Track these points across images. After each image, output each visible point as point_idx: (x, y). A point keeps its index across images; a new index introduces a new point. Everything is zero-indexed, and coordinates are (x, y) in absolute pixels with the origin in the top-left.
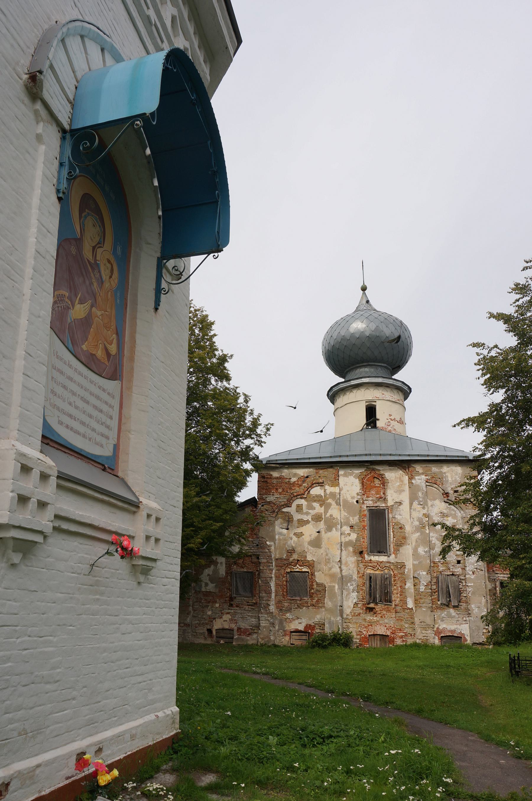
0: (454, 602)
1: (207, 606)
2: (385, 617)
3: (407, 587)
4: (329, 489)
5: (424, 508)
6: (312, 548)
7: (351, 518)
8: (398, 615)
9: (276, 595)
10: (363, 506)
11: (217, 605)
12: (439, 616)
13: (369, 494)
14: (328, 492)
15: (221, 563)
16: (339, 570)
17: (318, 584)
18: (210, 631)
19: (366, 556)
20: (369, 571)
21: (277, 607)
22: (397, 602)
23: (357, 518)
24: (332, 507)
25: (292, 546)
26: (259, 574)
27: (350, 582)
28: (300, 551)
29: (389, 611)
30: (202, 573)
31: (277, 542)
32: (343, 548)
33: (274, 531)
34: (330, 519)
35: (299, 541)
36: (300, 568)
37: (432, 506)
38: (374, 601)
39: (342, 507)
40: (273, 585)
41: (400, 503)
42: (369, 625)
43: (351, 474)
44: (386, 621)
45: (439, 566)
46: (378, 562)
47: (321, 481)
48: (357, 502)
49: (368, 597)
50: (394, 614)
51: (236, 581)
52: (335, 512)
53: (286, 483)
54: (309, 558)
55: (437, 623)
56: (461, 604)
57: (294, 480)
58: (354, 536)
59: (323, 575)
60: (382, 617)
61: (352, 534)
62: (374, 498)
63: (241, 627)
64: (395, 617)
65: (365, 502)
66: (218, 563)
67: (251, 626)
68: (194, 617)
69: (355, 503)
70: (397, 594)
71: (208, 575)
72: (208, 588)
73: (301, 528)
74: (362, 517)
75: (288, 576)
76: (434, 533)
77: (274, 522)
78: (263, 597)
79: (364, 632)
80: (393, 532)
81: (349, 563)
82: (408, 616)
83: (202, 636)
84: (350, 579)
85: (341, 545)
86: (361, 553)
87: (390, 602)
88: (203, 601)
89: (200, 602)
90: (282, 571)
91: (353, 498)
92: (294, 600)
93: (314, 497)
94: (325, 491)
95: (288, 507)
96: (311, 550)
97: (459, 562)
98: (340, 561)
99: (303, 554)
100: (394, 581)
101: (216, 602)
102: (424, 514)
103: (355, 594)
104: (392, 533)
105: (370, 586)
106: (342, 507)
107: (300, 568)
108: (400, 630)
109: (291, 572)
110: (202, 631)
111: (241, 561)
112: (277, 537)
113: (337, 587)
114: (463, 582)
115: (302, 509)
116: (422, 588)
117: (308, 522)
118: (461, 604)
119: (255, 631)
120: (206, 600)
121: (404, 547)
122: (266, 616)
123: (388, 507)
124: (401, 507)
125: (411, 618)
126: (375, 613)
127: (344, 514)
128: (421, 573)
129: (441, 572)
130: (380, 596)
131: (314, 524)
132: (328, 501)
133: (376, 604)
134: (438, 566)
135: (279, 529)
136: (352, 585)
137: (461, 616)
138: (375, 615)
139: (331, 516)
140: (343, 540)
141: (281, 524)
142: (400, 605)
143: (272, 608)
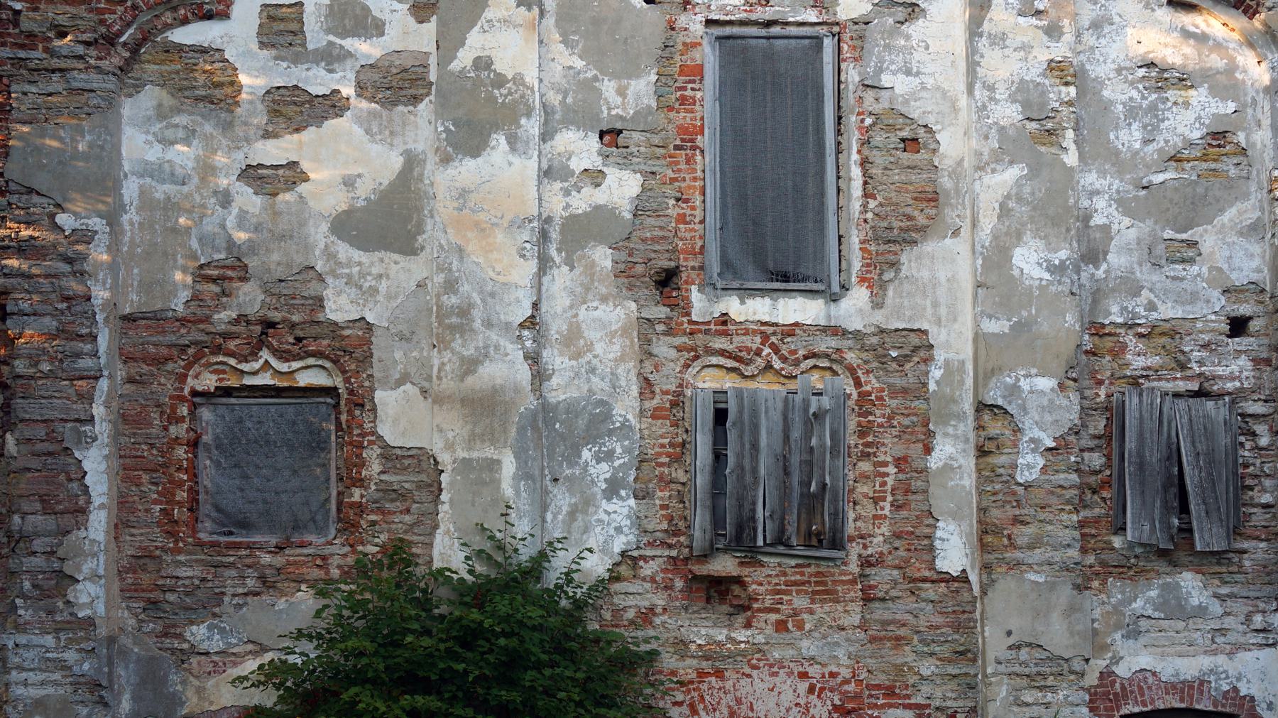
0: (1207, 536)
2: (800, 626)
3: (935, 461)
5: (1053, 32)
6: (357, 255)
7: (608, 88)
8: (879, 612)
9: (120, 526)
10: (682, 20)
16: (523, 373)
17: (391, 456)
19: (697, 298)
20: (710, 381)
21: (130, 593)
22: (877, 545)
23: (642, 89)
25: (231, 244)
27: (591, 437)
28: (280, 273)
29: (825, 592)
31: (130, 217)
32: (553, 252)
33: (108, 155)
34: (477, 82)
35: (277, 214)
36: (284, 367)
37: (1096, 26)
38: (738, 538)
39: (550, 21)
40: (96, 465)
42: (702, 674)
44: (808, 647)
45: (1124, 347)
46: (767, 332)
49: (701, 519)
50: (856, 608)
54: (340, 307)
55: (1104, 648)
56: (1246, 545)
58: (622, 188)
59: (422, 405)
60: (781, 626)
61: (613, 174)
64: (863, 626)
70: (876, 501)
74: (677, 76)
75: (206, 414)
76: (1102, 174)
77: (111, 104)
78: (24, 537)
80: (864, 163)
81: (592, 334)
82: (939, 620)
84: (596, 423)
85: (544, 236)
86: (666, 281)
87: (837, 542)
90: (165, 386)
92: (237, 546)
95: (209, 16)
97: (1238, 326)
98: (532, 322)
100: (862, 433)
102: (1055, 68)
103: (622, 509)
104: (856, 172)
105: (719, 457)
106: (550, 21)
107: (284, 367)
108: (890, 692)
109: (227, 392)
112: (130, 189)
113: (509, 466)
114: (1261, 428)
116: (1030, 465)
117: (332, 105)
118: (1246, 545)
121: (929, 247)
123: (837, 29)
124: (916, 29)
125: (957, 628)
126: (746, 608)
127: (566, 59)
128: (1025, 384)
129: (1134, 382)
133: (752, 555)
134: (1119, 351)
135: (147, 141)
136: (610, 456)
137: (1240, 608)
138: (740, 619)
139: (483, 63)
140: (557, 203)
141: (161, 114)
142: (889, 560)
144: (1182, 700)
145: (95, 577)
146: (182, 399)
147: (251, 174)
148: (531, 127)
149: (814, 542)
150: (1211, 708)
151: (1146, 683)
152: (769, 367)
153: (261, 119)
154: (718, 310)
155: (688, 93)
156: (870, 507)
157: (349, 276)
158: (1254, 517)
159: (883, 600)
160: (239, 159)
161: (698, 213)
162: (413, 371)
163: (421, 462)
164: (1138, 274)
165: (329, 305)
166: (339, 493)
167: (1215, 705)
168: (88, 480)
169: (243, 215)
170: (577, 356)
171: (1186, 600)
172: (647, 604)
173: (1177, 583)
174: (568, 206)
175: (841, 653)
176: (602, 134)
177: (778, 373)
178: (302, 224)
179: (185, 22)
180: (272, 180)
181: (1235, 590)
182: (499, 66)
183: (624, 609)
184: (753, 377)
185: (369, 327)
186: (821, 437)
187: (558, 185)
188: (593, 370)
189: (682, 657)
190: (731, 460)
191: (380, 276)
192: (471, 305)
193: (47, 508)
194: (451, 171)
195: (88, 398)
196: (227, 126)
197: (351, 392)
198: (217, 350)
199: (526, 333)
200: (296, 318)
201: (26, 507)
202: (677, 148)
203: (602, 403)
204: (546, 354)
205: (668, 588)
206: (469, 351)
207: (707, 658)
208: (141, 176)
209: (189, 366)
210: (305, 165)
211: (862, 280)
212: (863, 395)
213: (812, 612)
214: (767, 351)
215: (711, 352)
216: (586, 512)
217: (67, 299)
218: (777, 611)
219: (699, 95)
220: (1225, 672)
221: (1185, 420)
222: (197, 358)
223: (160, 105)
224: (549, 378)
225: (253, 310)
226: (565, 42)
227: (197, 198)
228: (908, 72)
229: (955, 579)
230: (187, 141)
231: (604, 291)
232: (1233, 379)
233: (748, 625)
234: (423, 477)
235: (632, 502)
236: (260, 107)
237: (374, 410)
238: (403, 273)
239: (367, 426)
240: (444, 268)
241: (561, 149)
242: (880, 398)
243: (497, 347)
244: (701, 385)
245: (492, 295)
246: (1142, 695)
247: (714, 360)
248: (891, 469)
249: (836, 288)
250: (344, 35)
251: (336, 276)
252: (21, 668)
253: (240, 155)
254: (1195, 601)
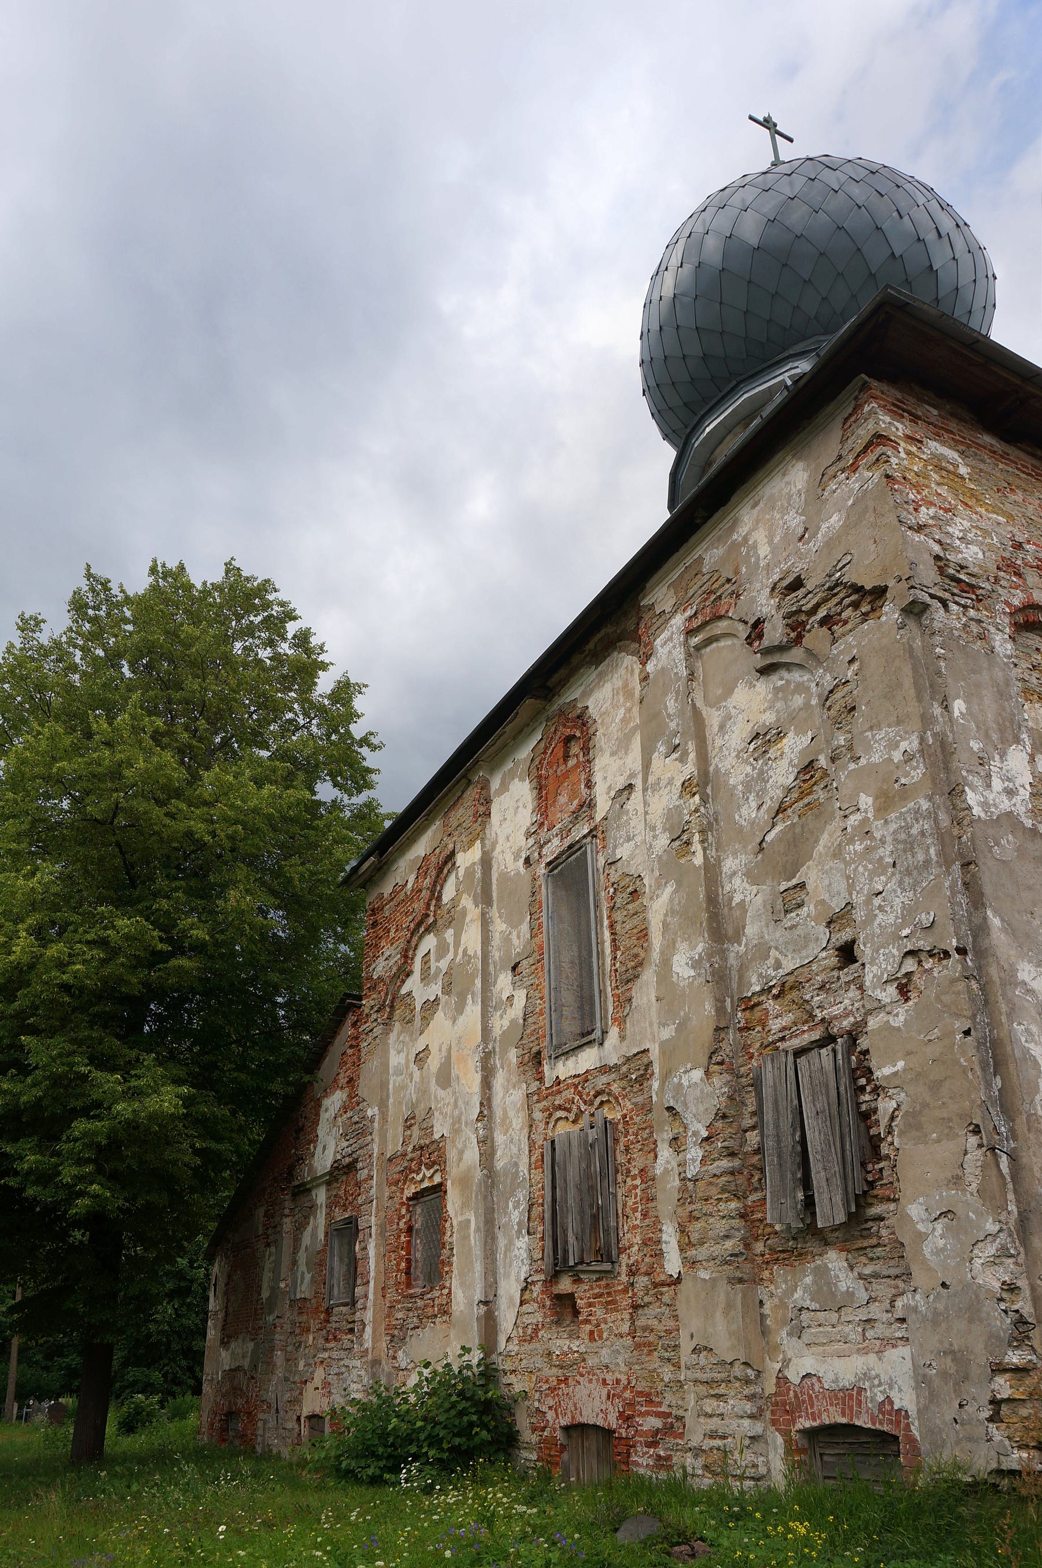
12: (783, 1305)
41: (630, 787)
144: (843, 1415)
150: (869, 1426)
151: (813, 1389)
158: (885, 1173)
164: (766, 937)
167: (874, 1424)
171: (835, 1285)
173: (826, 1264)
181: (877, 1268)
220: (878, 1376)
221: (808, 1074)
228: (629, 839)
232: (847, 1016)
246: (812, 1407)
254: (843, 1287)
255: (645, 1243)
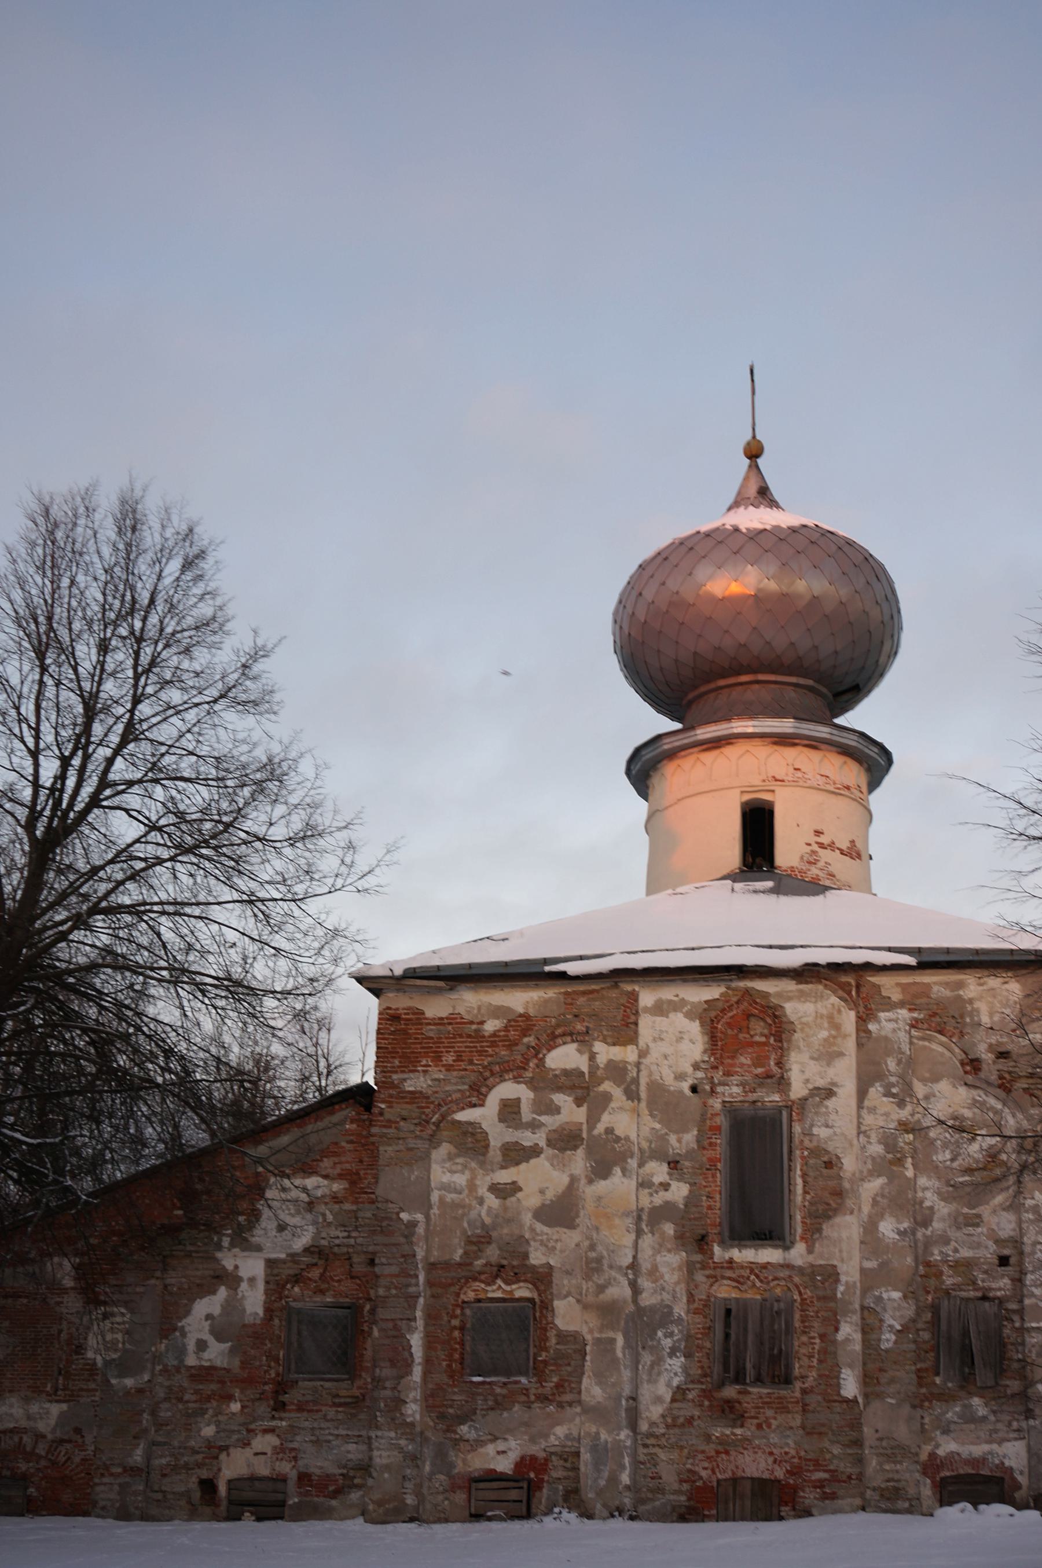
1: (203, 1412)
2: (769, 1426)
4: (605, 1052)
6: (546, 1229)
7: (673, 1139)
9: (426, 1374)
10: (711, 1101)
11: (235, 1407)
13: (732, 1065)
14: (602, 1060)
15: (252, 1280)
16: (628, 1292)
17: (563, 1337)
18: (208, 1486)
19: (717, 1249)
22: (810, 1382)
23: (690, 1138)
24: (613, 1105)
26: (372, 1312)
27: (662, 1324)
29: (782, 1407)
30: (188, 1313)
31: (435, 1211)
32: (644, 1227)
35: (506, 1209)
40: (416, 1341)
42: (718, 1452)
43: (675, 1006)
44: (774, 1438)
47: (579, 1027)
48: (694, 1089)
49: (717, 1369)
51: (299, 1333)
52: (623, 1120)
53: (469, 1036)
54: (537, 1258)
57: (491, 1026)
58: (679, 1191)
59: (578, 1307)
60: (759, 1426)
61: (674, 1185)
62: (748, 1078)
63: (312, 1470)
65: (719, 1089)
66: (240, 1279)
67: (345, 1467)
68: (154, 1443)
69: (688, 1092)
70: (810, 1357)
71: (209, 1317)
72: (206, 1355)
73: (513, 1170)
74: (707, 1132)
79: (704, 1474)
81: (663, 1270)
83: (183, 1503)
84: (663, 1316)
85: (639, 1218)
86: (702, 1242)
88: (187, 1397)
89: (180, 1400)
91: (680, 1077)
93: (556, 1076)
94: (592, 1057)
95: (475, 1106)
96: (542, 1233)
98: (634, 1266)
99: (517, 1249)
100: (803, 1322)
101: (230, 1398)
103: (676, 1363)
105: (727, 1336)
106: (643, 1104)
110: (181, 1488)
111: (315, 1273)
112: (435, 1197)
115: (519, 1113)
117: (535, 1152)
119: (357, 1481)
120: (196, 1392)
122: (392, 1434)
127: (651, 1124)
130: (757, 1368)
131: (555, 1156)
132: (601, 1088)
136: (671, 1335)
138: (739, 1422)
139: (609, 1131)
140: (645, 1201)
141: (450, 1158)
143: (413, 1410)
145: (415, 1401)
146: (457, 1306)
147: (494, 1188)
148: (633, 1163)
149: (777, 1380)
152: (754, 1285)
153: (499, 1158)
154: (727, 1256)
155: (714, 1140)
156: (806, 1359)
157: (542, 1241)
159: (813, 1412)
160: (488, 1180)
161: (718, 1205)
162: (573, 1290)
163: (573, 1338)
165: (532, 1256)
166: (535, 1354)
168: (413, 1350)
169: (490, 1208)
170: (655, 1281)
172: (690, 1414)
174: (652, 1202)
175: (790, 1442)
176: (669, 1163)
177: (758, 1288)
178: (519, 1213)
179: (463, 1109)
180: (506, 1191)
182: (617, 1132)
183: (678, 1417)
184: (746, 1291)
185: (551, 1267)
186: (780, 1324)
187: (647, 1191)
188: (663, 1289)
189: (708, 1443)
190: (733, 1337)
191: (557, 1240)
192: (602, 1257)
193: (393, 1363)
194: (593, 1187)
195: (413, 1307)
196: (482, 1164)
197: (542, 1302)
198: (475, 1279)
199: (630, 1271)
200: (515, 1263)
201: (382, 1364)
202: (708, 1169)
203: (668, 1306)
204: (639, 1281)
205: (701, 1405)
206: (601, 1282)
207: (720, 1444)
208: (439, 1190)
209: (460, 1289)
210: (521, 1183)
211: (802, 1238)
212: (803, 1300)
213: (775, 1418)
214: (753, 1277)
215: (723, 1277)
216: (659, 1365)
217: (403, 1256)
218: (757, 1418)
219: (719, 1141)
222: (466, 1284)
223: (449, 1154)
224: (641, 1293)
225: (494, 1260)
226: (651, 1115)
227: (467, 1200)
229: (851, 1401)
230: (462, 1172)
231: (669, 1246)
233: (742, 1426)
234: (577, 1347)
235: (683, 1359)
236: (499, 1152)
237: (553, 1310)
238: (571, 1238)
239: (550, 1319)
240: (589, 1238)
241: (648, 1172)
242: (812, 1302)
243: (615, 1279)
244: (719, 1295)
245: (613, 1252)
247: (725, 1282)
248: (817, 1341)
249: (788, 1243)
250: (539, 1115)
251: (535, 1241)
252: (379, 1449)
253: (488, 1178)
255: (820, 1376)
